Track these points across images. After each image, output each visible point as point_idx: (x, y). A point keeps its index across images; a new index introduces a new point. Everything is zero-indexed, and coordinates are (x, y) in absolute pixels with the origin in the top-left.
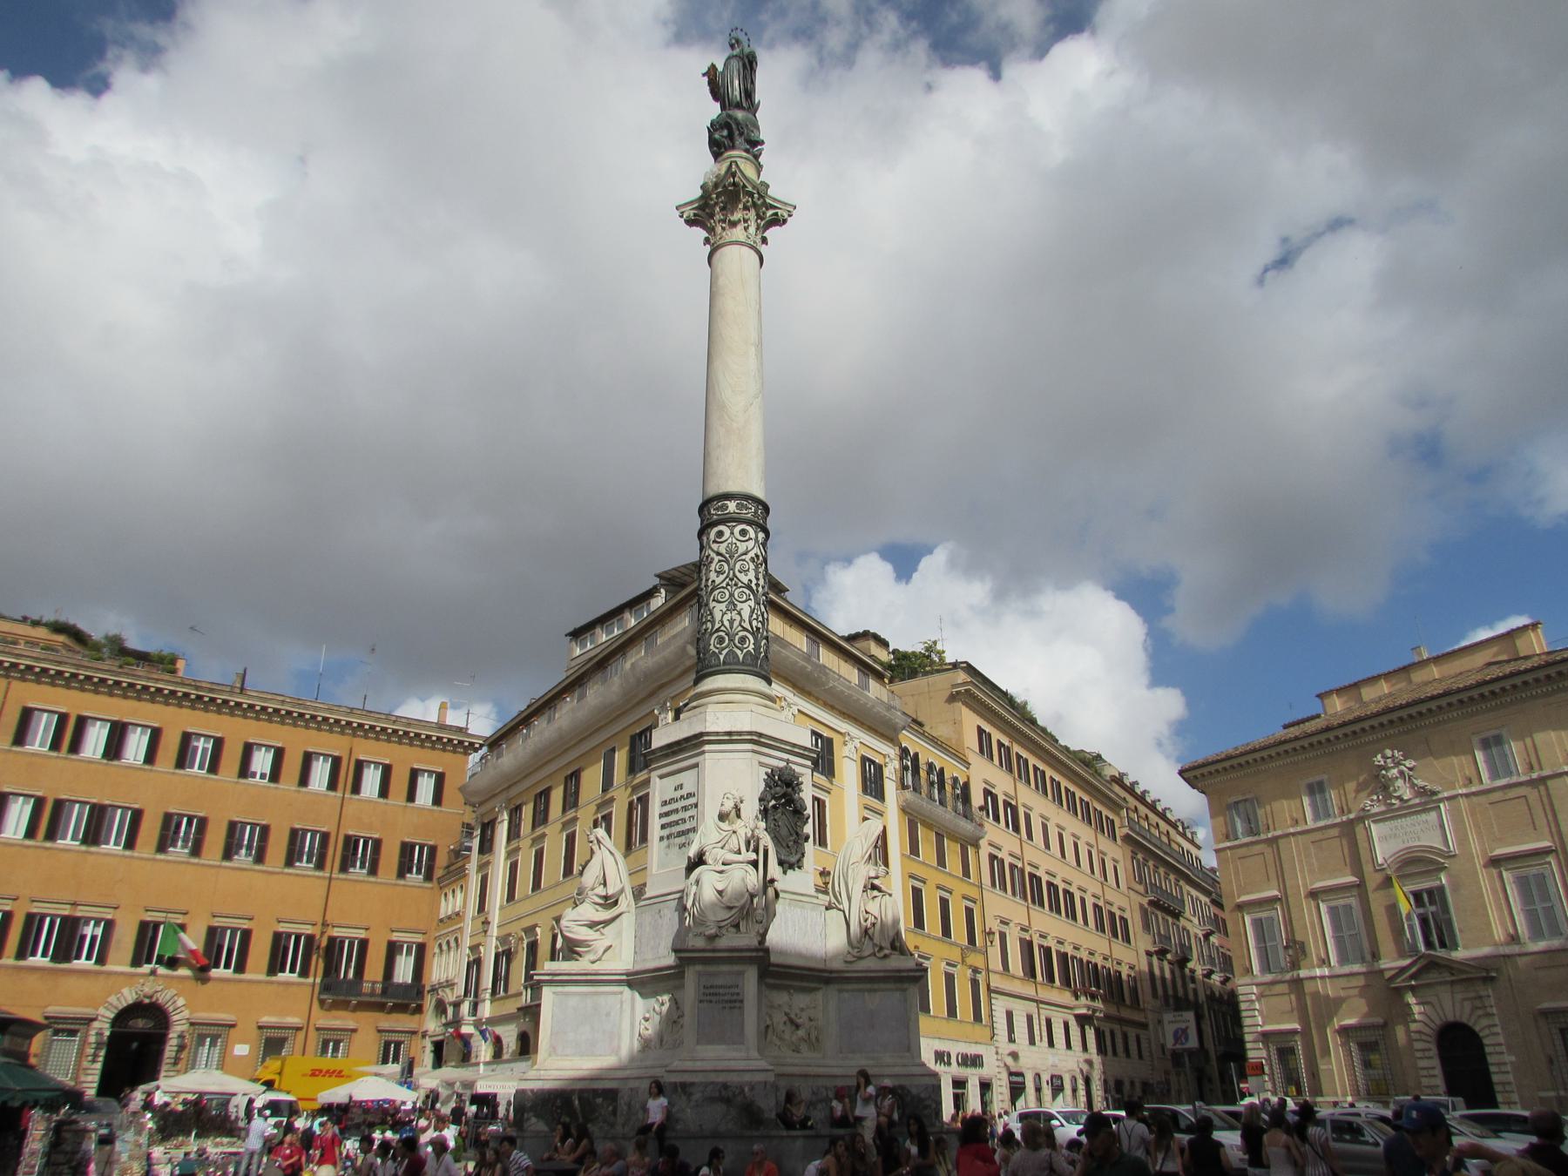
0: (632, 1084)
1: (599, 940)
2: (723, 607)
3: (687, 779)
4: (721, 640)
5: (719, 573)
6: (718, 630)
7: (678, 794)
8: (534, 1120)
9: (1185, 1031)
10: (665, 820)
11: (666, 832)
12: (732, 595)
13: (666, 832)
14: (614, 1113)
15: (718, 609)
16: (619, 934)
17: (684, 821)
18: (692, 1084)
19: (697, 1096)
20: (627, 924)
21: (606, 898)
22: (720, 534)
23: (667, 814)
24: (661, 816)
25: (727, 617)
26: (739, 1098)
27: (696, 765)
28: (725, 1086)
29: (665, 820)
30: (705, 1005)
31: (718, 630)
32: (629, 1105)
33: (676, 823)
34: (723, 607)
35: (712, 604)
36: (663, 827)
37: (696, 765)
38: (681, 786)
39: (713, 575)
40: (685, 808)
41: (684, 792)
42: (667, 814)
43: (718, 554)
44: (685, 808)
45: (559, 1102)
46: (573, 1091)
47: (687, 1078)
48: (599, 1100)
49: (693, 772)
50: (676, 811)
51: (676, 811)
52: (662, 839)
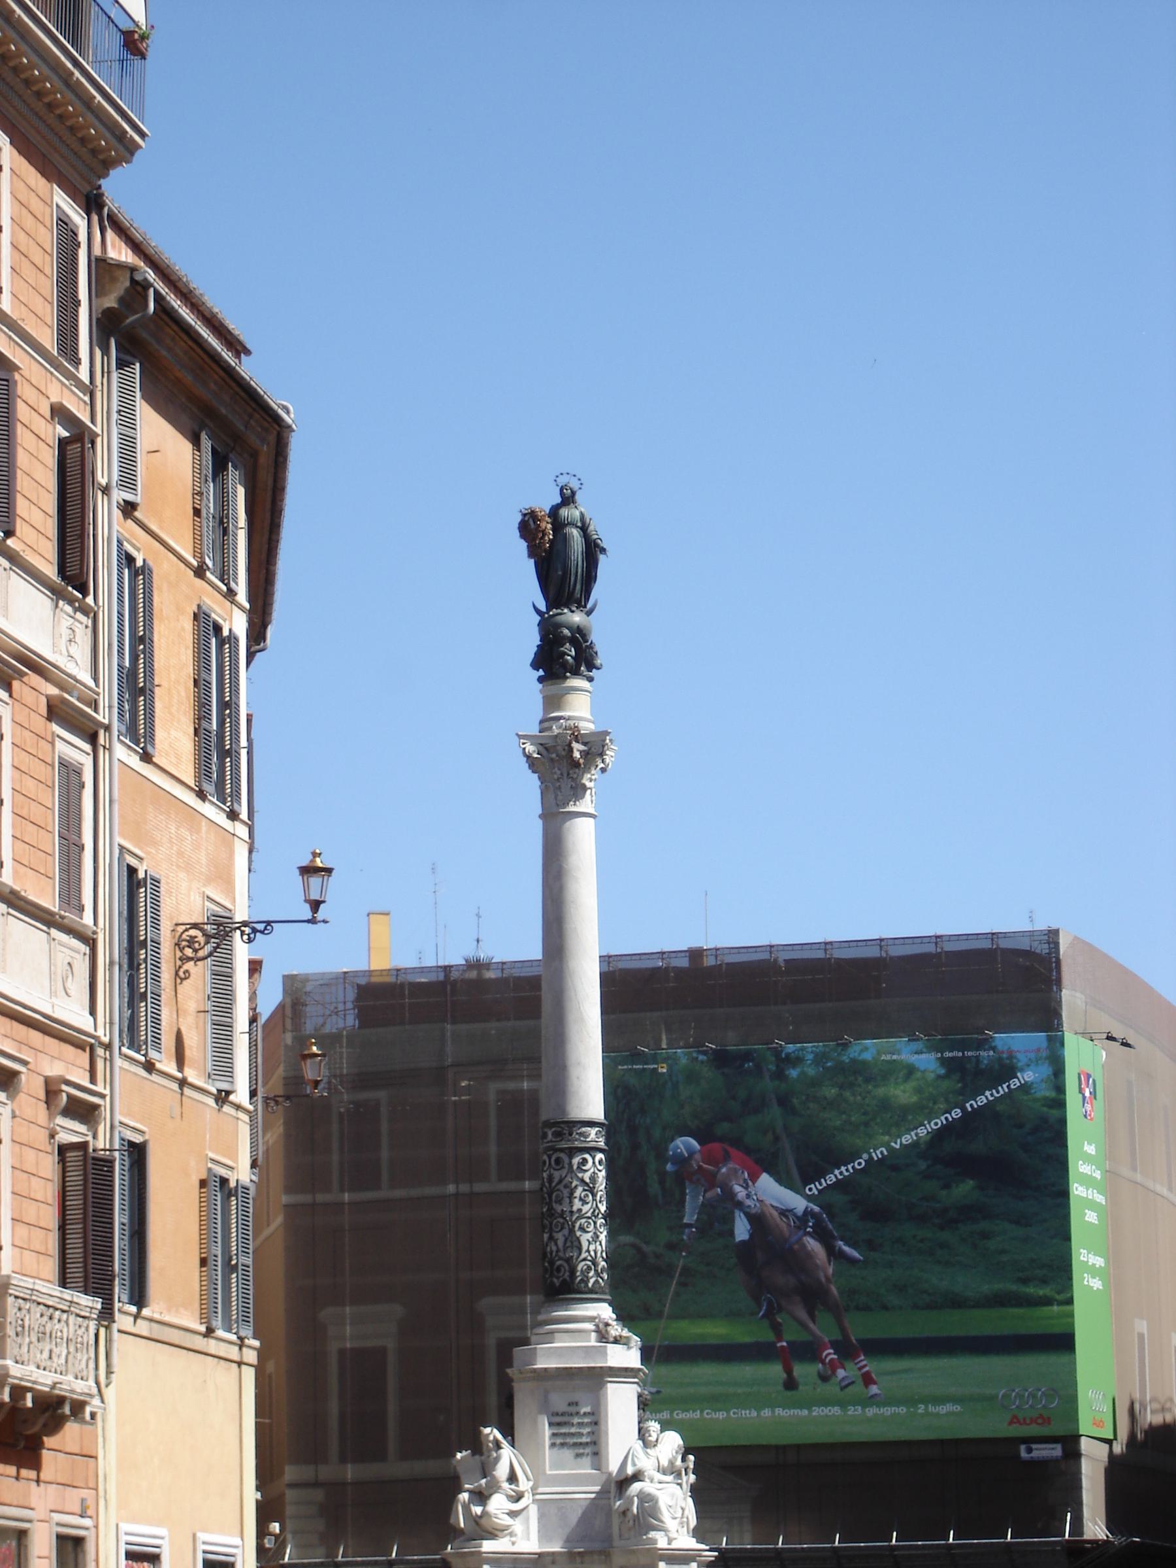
1: (517, 1525)
2: (589, 1236)
4: (589, 1268)
5: (584, 1202)
6: (585, 1259)
7: (573, 1409)
11: (558, 1441)
12: (595, 1223)
13: (558, 1441)
15: (585, 1238)
16: (527, 1519)
17: (581, 1435)
20: (533, 1511)
22: (585, 1161)
25: (592, 1247)
31: (585, 1259)
33: (573, 1435)
34: (589, 1236)
35: (578, 1233)
39: (577, 1204)
40: (580, 1424)
42: (559, 1424)
43: (582, 1181)
44: (580, 1424)
52: (553, 1445)
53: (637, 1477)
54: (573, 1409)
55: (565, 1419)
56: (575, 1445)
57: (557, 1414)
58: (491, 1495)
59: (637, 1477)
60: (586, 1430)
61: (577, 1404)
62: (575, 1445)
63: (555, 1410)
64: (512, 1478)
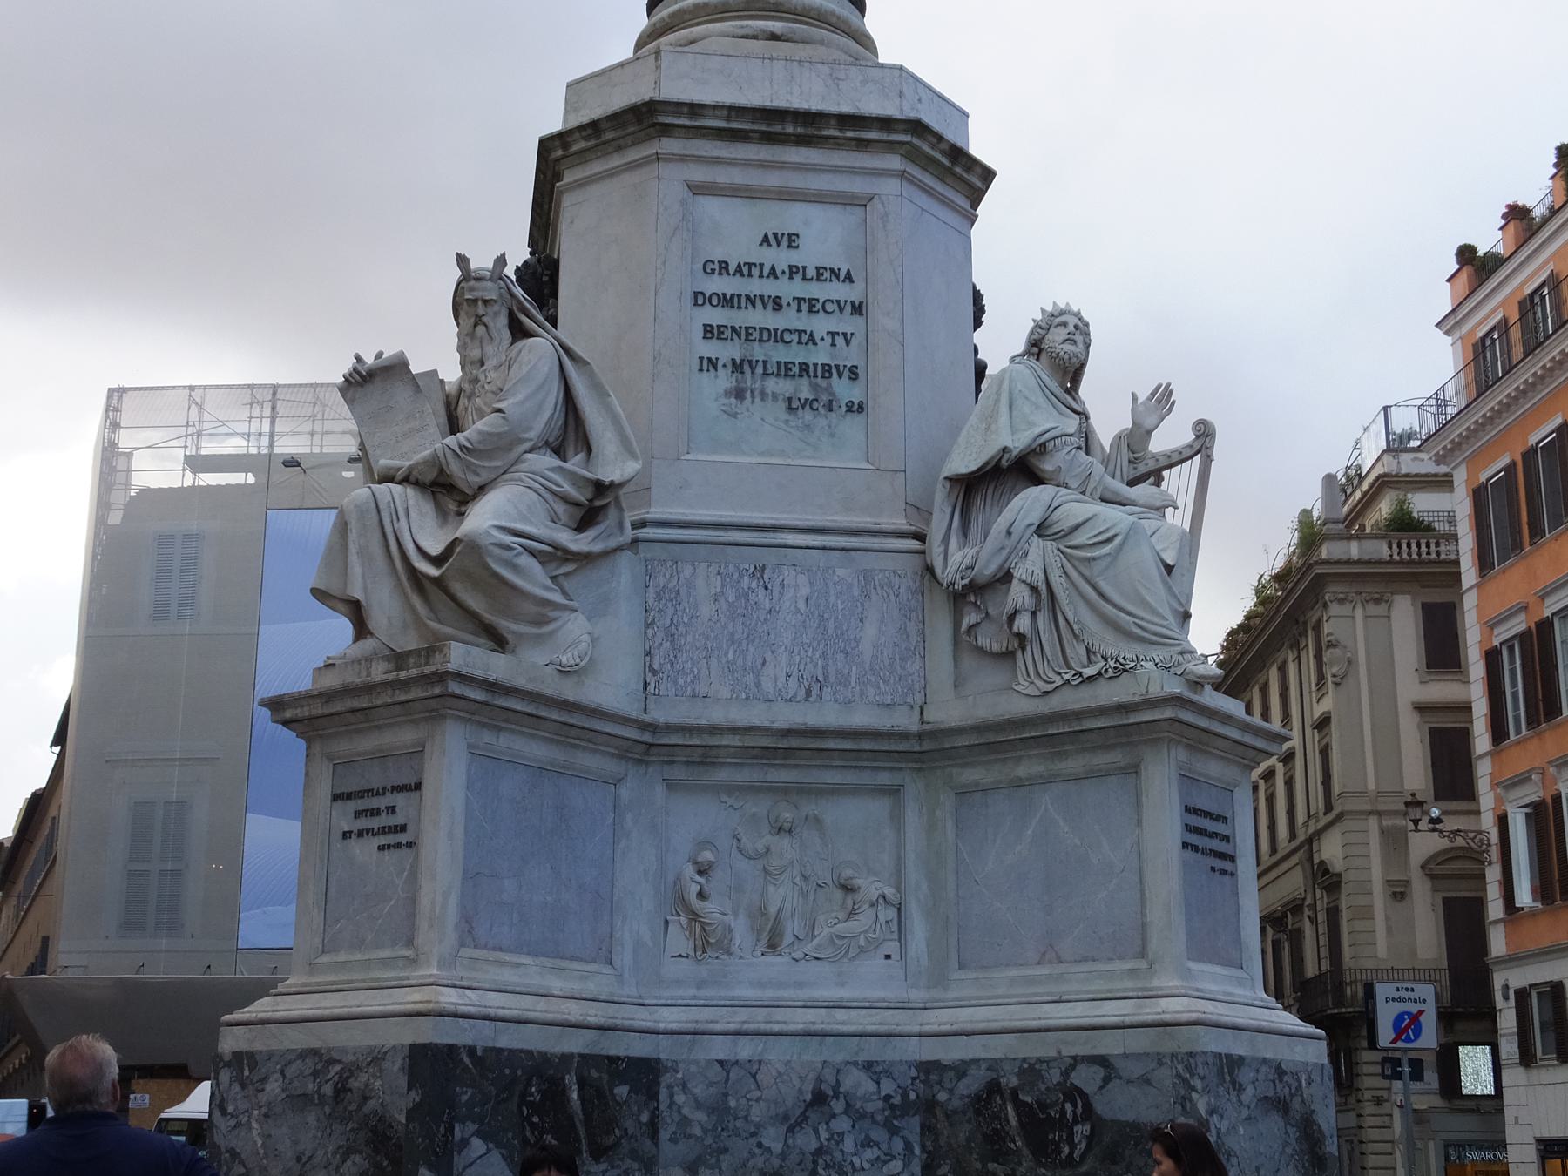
0: (719, 1049)
3: (823, 236)
7: (781, 258)
8: (478, 1146)
9: (1415, 1018)
10: (717, 316)
11: (727, 351)
14: (653, 1129)
18: (1241, 1060)
19: (1249, 1094)
21: (600, 488)
23: (727, 301)
24: (700, 299)
26: (1297, 1101)
27: (861, 202)
28: (1280, 1072)
29: (717, 316)
30: (1189, 854)
32: (719, 1109)
33: (778, 337)
36: (709, 332)
37: (861, 202)
38: (792, 241)
41: (810, 255)
42: (727, 301)
44: (812, 306)
45: (535, 1094)
46: (566, 1058)
47: (1237, 1046)
48: (622, 1091)
49: (853, 216)
50: (777, 304)
51: (777, 304)
53: (1022, 469)
54: (781, 258)
55: (756, 287)
56: (785, 370)
57: (724, 267)
58: (482, 489)
59: (1022, 469)
60: (820, 325)
61: (792, 241)
62: (785, 370)
63: (718, 255)
64: (571, 433)
